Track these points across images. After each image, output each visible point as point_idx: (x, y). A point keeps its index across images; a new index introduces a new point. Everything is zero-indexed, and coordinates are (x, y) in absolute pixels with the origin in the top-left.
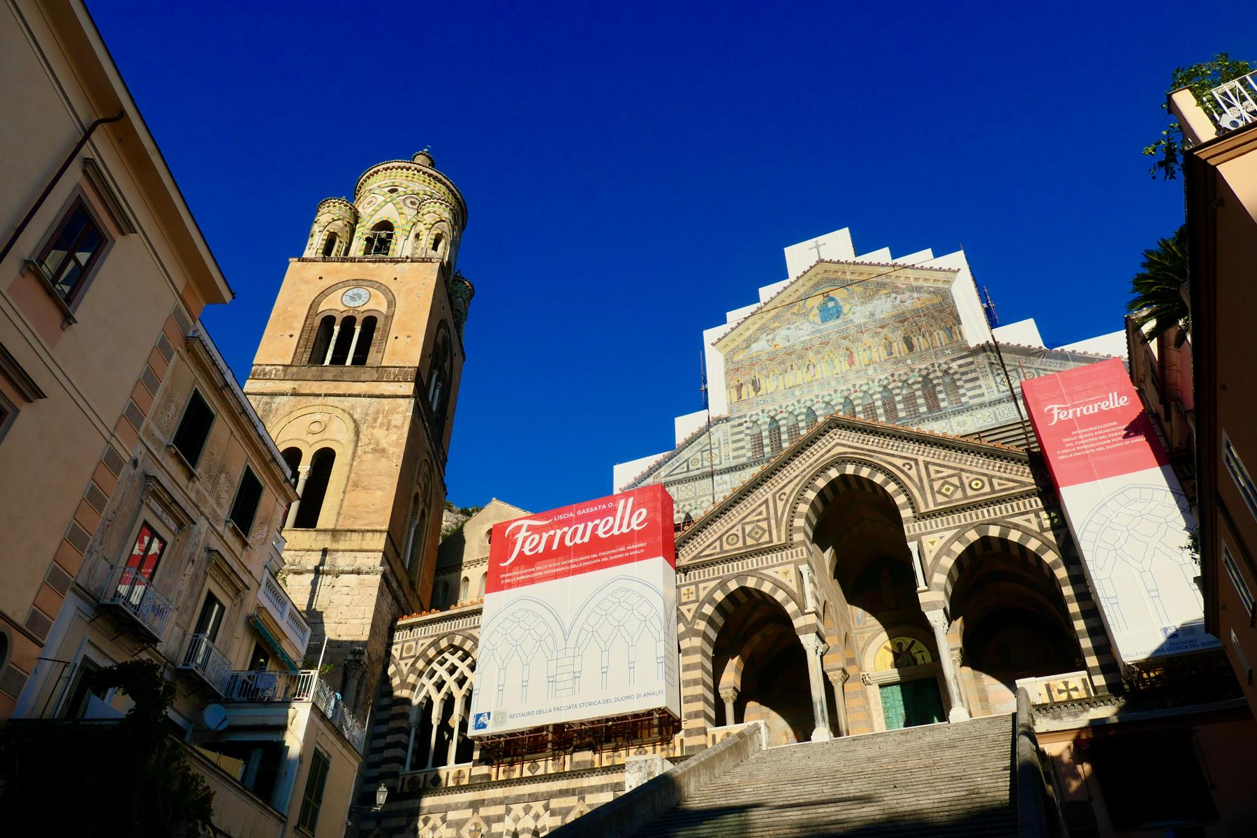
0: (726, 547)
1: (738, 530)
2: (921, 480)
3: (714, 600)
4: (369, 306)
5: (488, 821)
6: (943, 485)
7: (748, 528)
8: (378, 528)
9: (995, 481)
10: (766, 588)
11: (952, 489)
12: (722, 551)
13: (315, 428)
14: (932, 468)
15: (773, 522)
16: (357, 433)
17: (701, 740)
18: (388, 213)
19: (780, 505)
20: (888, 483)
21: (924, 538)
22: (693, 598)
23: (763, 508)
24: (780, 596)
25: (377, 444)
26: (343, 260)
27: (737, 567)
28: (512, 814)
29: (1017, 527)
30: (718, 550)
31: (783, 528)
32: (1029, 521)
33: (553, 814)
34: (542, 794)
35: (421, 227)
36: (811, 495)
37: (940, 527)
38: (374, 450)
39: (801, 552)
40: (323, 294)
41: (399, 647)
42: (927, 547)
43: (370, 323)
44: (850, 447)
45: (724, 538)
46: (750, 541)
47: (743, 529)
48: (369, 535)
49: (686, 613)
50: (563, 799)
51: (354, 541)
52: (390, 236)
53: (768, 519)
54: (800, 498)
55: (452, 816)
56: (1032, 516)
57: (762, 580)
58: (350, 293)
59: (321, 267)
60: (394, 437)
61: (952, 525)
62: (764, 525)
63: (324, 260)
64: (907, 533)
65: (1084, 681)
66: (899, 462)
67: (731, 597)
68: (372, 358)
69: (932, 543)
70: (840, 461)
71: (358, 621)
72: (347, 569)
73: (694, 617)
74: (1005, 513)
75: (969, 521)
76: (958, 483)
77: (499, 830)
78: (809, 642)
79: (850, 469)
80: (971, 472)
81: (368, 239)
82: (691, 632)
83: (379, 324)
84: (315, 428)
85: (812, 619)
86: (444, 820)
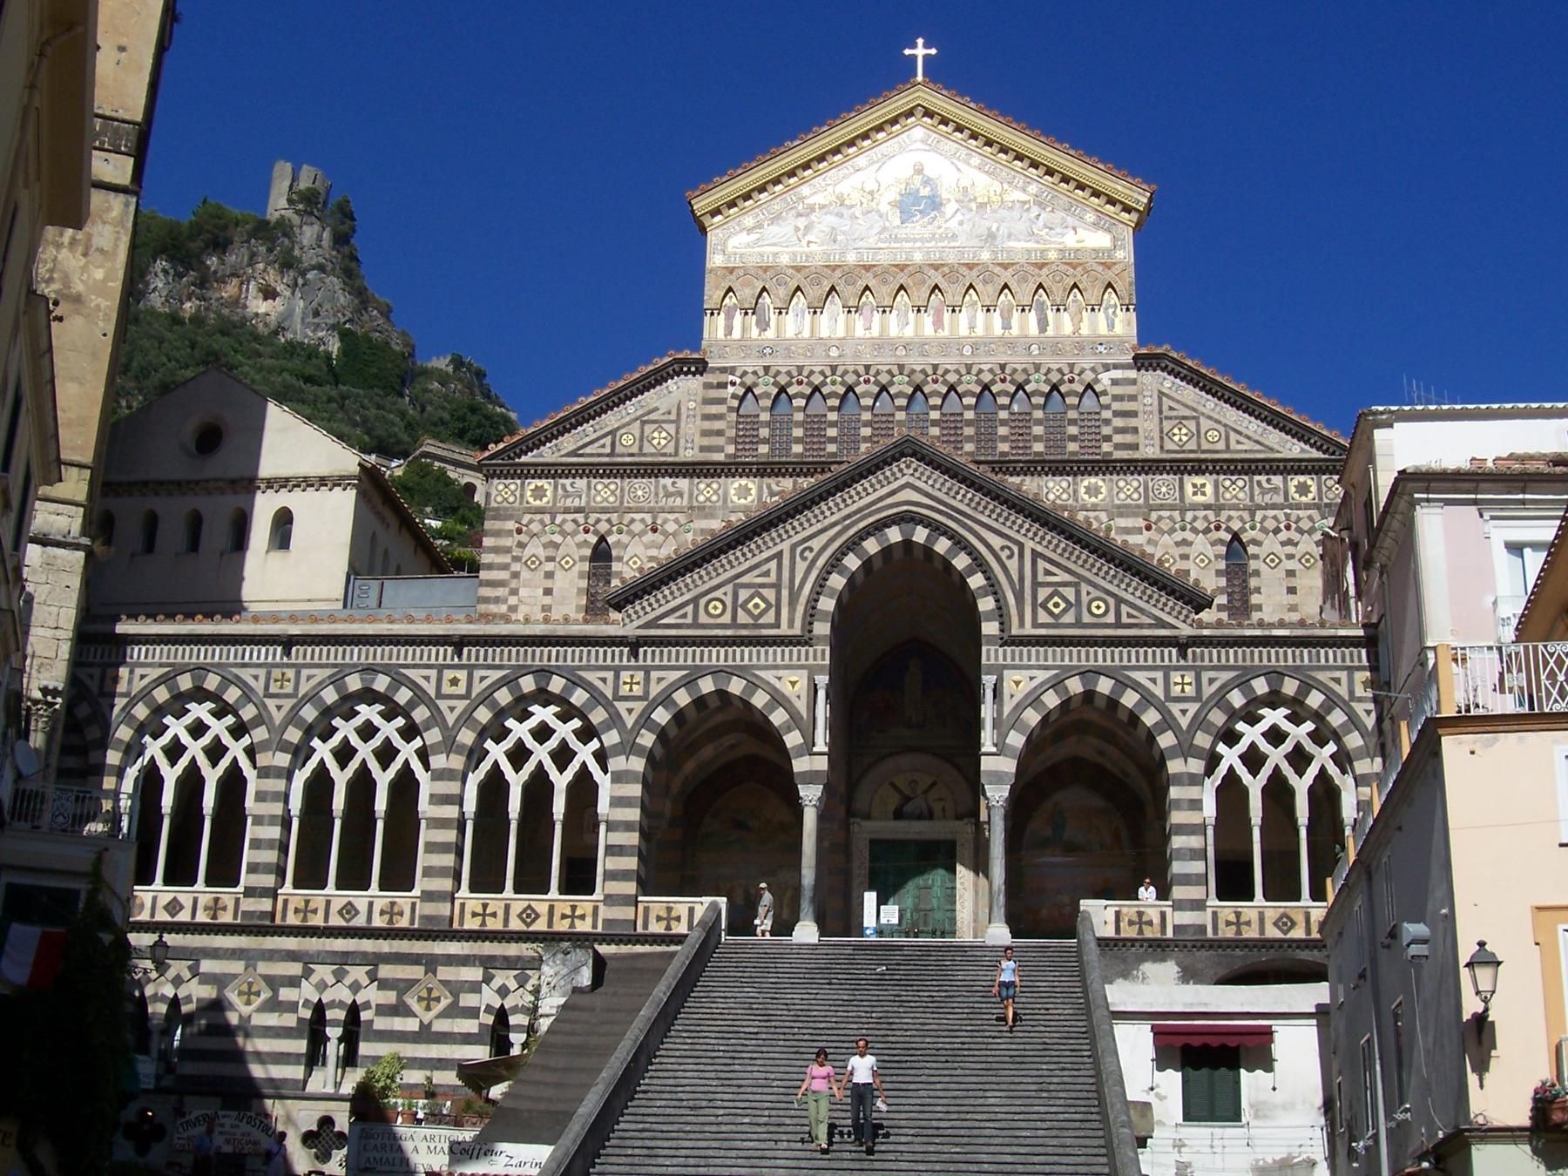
0: (703, 618)
1: (726, 593)
2: (1022, 579)
3: (675, 703)
5: (274, 982)
6: (1051, 597)
7: (743, 595)
9: (1124, 609)
10: (759, 700)
11: (1063, 605)
12: (695, 624)
14: (1041, 564)
15: (785, 593)
17: (627, 913)
19: (801, 567)
20: (972, 573)
21: (1006, 672)
22: (638, 690)
23: (773, 565)
24: (778, 718)
25: (67, 282)
27: (716, 657)
28: (314, 979)
29: (1137, 686)
30: (689, 620)
31: (800, 609)
32: (1154, 681)
33: (384, 985)
34: (365, 954)
36: (852, 562)
37: (1033, 662)
39: (822, 654)
41: (96, 671)
42: (1008, 686)
44: (927, 495)
45: (703, 601)
46: (743, 618)
47: (735, 596)
49: (624, 714)
50: (400, 968)
53: (777, 586)
54: (835, 564)
55: (207, 966)
56: (1159, 675)
57: (753, 686)
60: (99, 274)
61: (1050, 662)
62: (770, 594)
64: (984, 661)
65: (1163, 915)
66: (996, 542)
67: (700, 702)
69: (1017, 683)
70: (907, 519)
71: (50, 633)
73: (636, 722)
74: (1125, 663)
75: (1075, 662)
76: (1072, 599)
77: (295, 999)
78: (810, 794)
79: (920, 535)
80: (1095, 586)
82: (628, 747)
85: (822, 764)
86: (195, 972)
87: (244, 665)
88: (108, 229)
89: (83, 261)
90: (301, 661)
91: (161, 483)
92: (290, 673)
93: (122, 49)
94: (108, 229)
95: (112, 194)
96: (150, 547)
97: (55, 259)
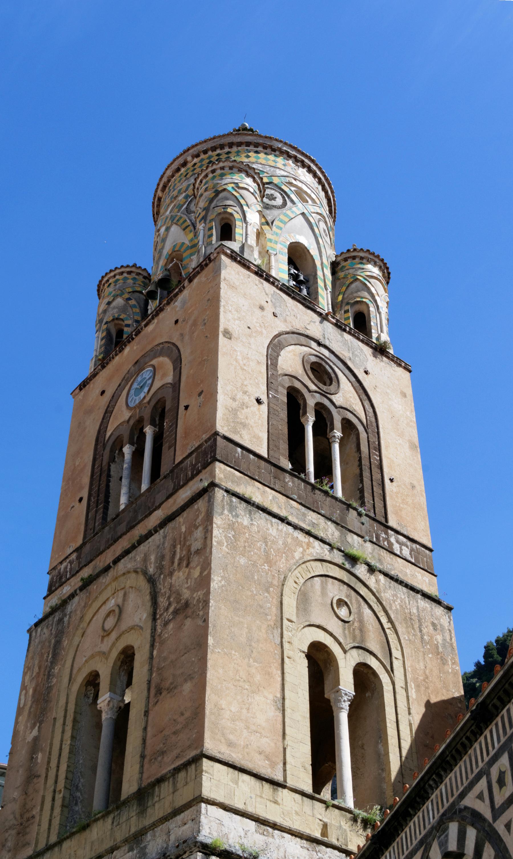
8: (193, 753)
38: (176, 612)
40: (108, 412)
48: (182, 775)
58: (135, 386)
60: (196, 573)
89: (187, 570)
94: (200, 529)
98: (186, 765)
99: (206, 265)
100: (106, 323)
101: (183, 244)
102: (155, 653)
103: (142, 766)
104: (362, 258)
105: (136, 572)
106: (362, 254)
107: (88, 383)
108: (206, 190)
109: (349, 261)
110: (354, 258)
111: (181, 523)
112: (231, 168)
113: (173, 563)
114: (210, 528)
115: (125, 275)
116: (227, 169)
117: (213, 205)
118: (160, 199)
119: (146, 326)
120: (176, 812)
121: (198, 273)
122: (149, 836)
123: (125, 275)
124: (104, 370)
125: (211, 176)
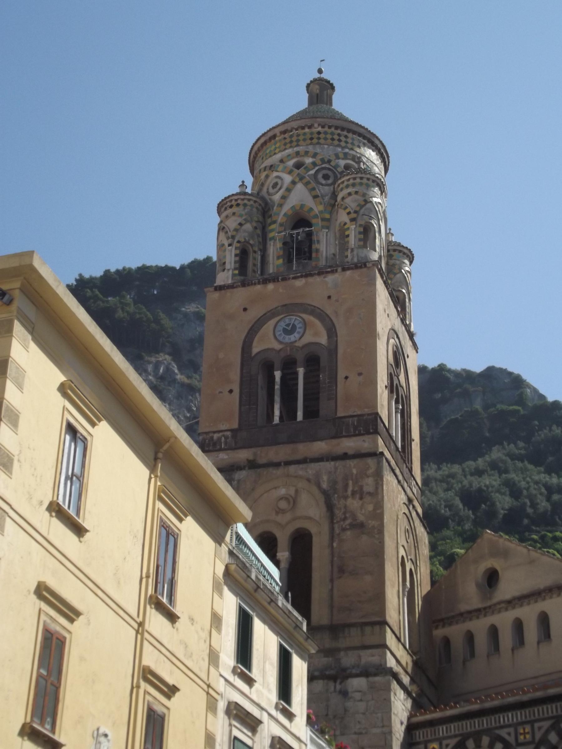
4: (308, 338)
8: (377, 619)
13: (283, 505)
16: (330, 507)
18: (300, 196)
26: (265, 281)
35: (343, 217)
43: (313, 361)
48: (368, 629)
51: (353, 637)
52: (309, 235)
59: (241, 295)
60: (370, 507)
63: (244, 284)
68: (325, 408)
72: (354, 671)
81: (285, 244)
83: (324, 362)
84: (283, 505)
87: (502, 727)
88: (370, 481)
89: (361, 502)
90: (532, 718)
91: (470, 612)
92: (528, 729)
93: (360, 374)
95: (371, 461)
96: (472, 654)
97: (345, 507)
98: (373, 624)
99: (361, 267)
100: (239, 242)
101: (311, 209)
102: (335, 545)
103: (332, 611)
104: (404, 254)
105: (309, 480)
106: (406, 251)
107: (224, 289)
108: (356, 193)
109: (396, 253)
110: (400, 251)
111: (353, 466)
112: (374, 181)
113: (346, 491)
114: (381, 483)
115: (252, 202)
116: (371, 181)
117: (362, 211)
118: (274, 137)
119: (294, 278)
120: (365, 647)
121: (352, 269)
122: (342, 653)
123: (252, 202)
124: (243, 289)
125: (358, 180)
